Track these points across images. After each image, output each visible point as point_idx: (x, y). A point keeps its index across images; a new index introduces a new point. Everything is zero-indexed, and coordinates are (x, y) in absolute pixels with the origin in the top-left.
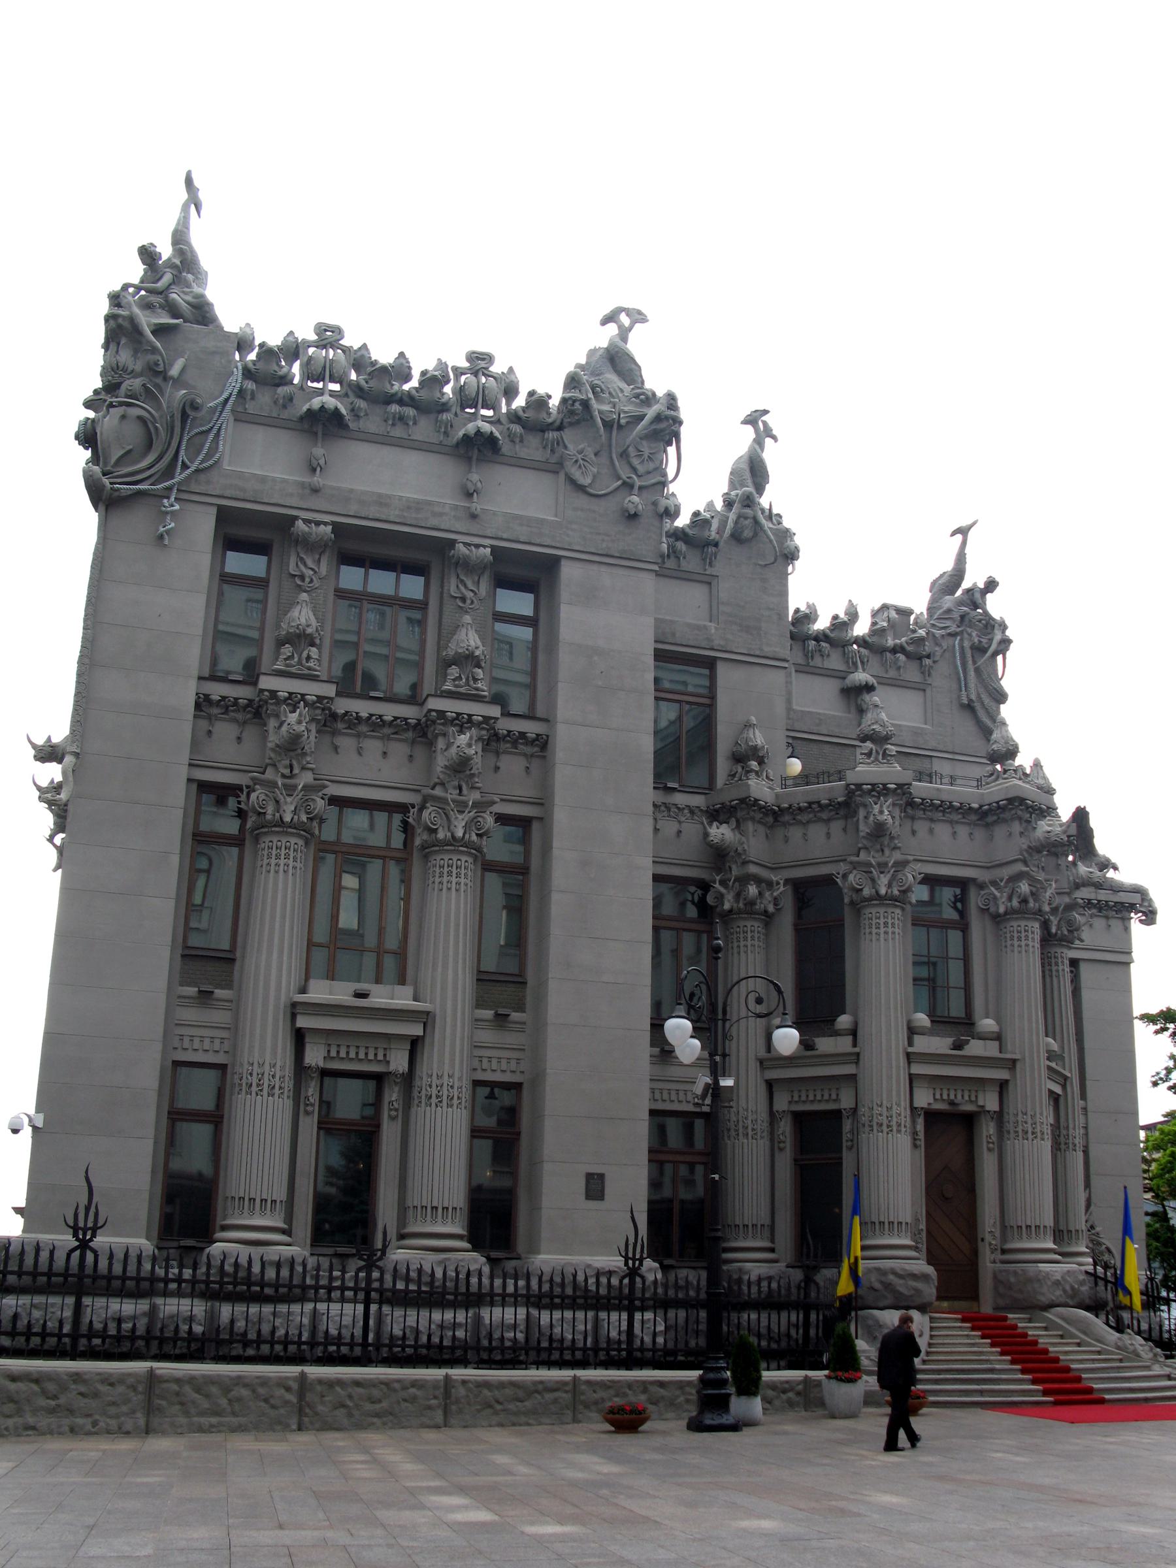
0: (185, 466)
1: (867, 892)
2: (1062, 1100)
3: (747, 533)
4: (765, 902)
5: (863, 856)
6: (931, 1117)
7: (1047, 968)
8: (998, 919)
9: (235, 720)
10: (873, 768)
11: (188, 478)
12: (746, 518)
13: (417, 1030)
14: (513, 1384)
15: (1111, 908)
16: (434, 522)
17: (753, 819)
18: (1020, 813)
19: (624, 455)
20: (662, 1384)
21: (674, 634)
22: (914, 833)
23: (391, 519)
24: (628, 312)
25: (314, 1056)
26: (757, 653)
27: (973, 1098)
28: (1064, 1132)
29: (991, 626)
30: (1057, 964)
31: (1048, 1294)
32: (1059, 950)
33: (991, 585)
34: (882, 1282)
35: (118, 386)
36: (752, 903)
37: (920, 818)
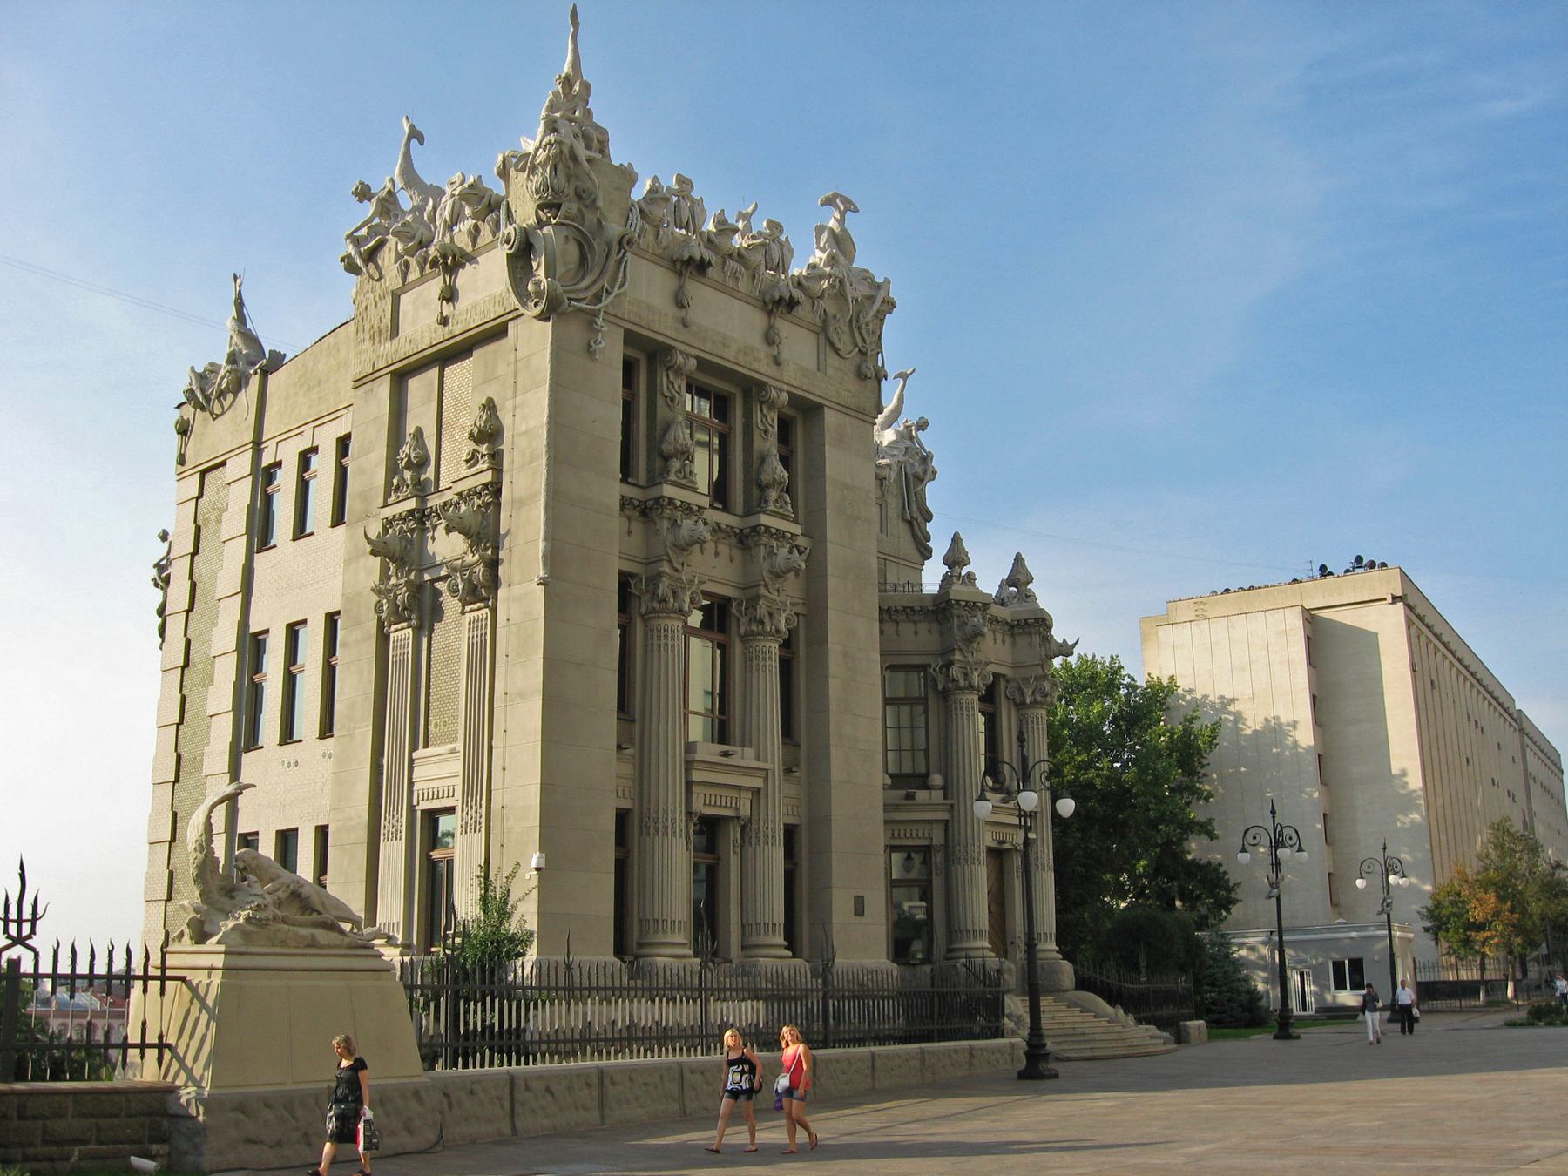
0: (608, 293)
5: (958, 656)
6: (990, 850)
8: (1020, 706)
9: (629, 519)
10: (963, 588)
11: (612, 303)
13: (758, 783)
14: (899, 1056)
16: (755, 366)
19: (859, 328)
20: (956, 1051)
23: (729, 357)
24: (846, 201)
25: (699, 806)
29: (926, 459)
33: (922, 425)
35: (559, 207)
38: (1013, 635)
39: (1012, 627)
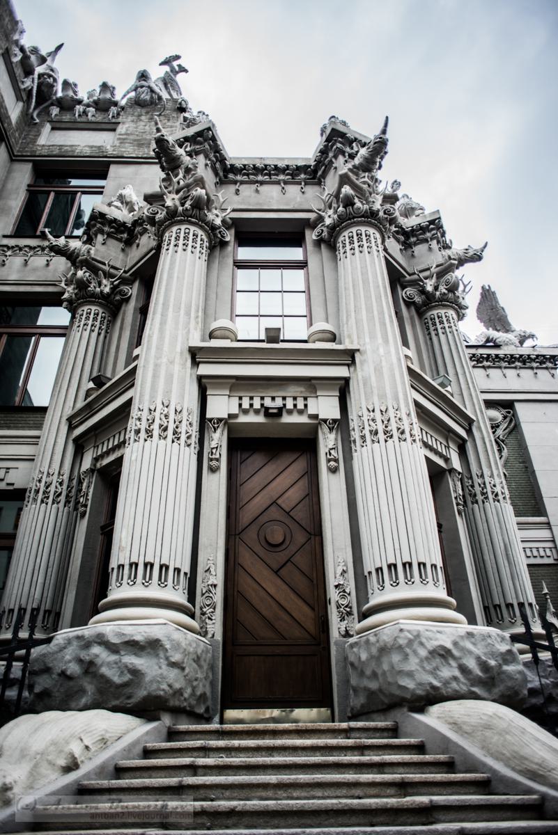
1: (160, 216)
2: (469, 446)
3: (146, 96)
4: (102, 287)
7: (432, 328)
12: (142, 87)
15: (534, 360)
17: (102, 232)
18: (339, 145)
21: (73, 151)
22: (237, 192)
26: (145, 156)
27: (300, 406)
28: (477, 481)
30: (441, 322)
31: (416, 674)
32: (442, 312)
34: (80, 661)
36: (82, 285)
37: (242, 183)
38: (319, 183)
39: (315, 171)
